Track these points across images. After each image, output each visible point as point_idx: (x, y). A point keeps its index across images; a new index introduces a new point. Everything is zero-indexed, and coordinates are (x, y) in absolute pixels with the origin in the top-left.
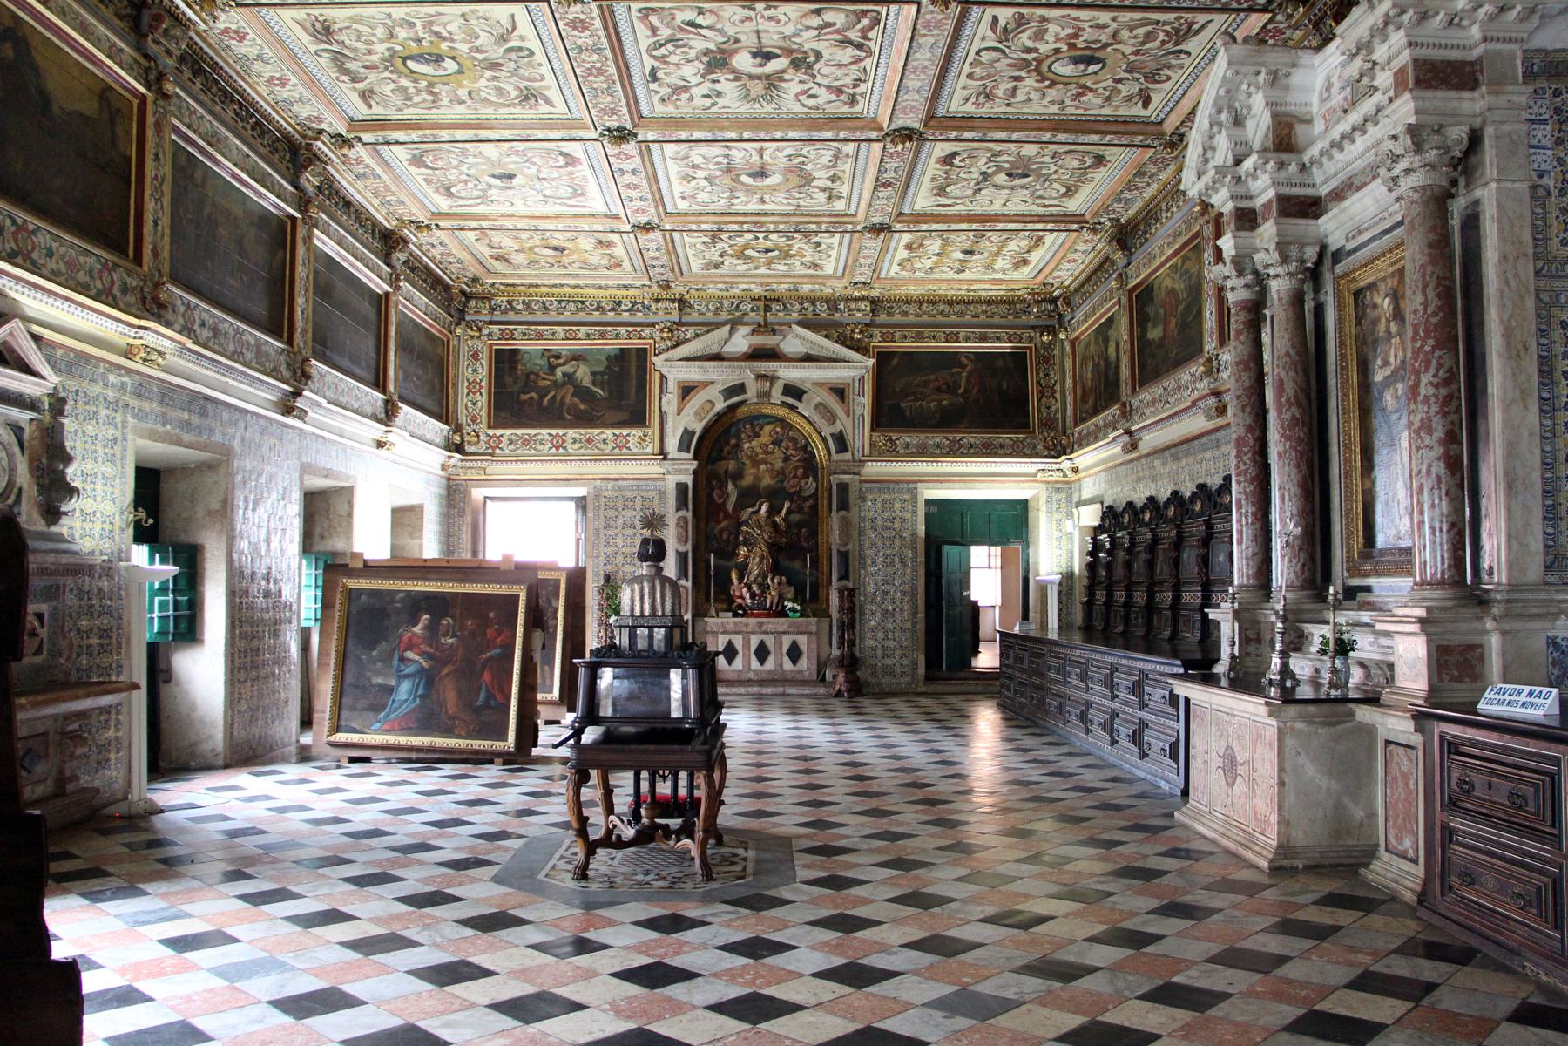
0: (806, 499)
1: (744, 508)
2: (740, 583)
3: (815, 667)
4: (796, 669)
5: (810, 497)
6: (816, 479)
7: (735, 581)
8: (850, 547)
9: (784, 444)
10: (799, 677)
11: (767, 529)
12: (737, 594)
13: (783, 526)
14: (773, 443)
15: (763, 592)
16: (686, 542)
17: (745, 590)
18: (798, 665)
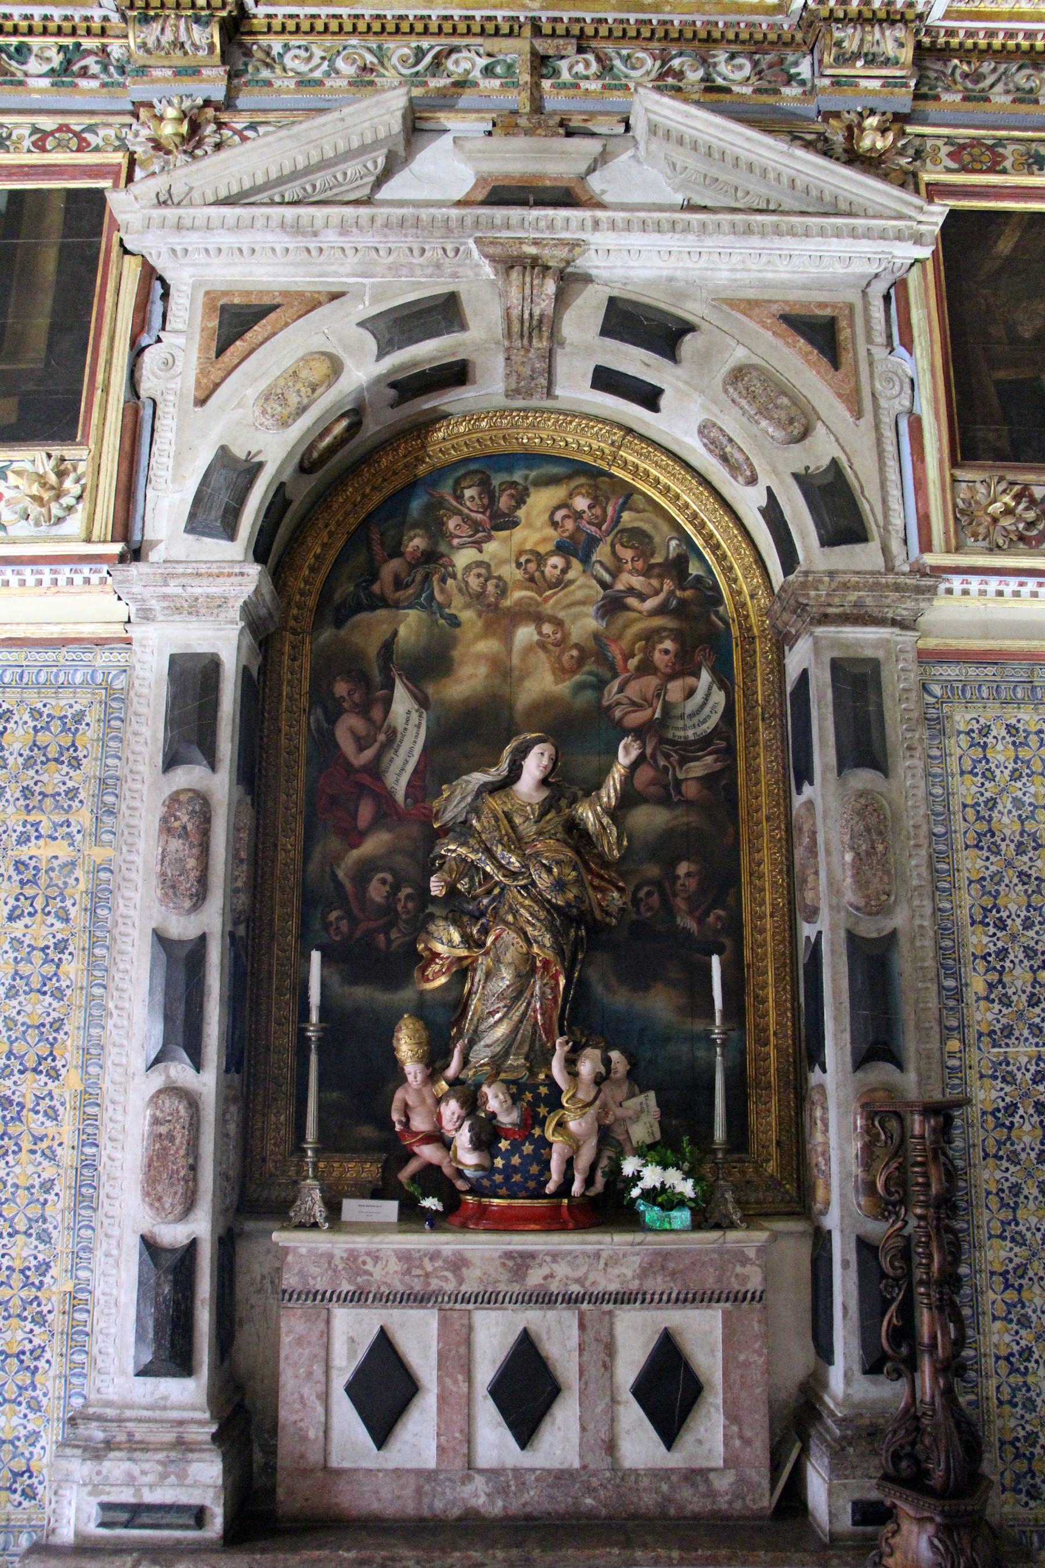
0: (688, 751)
1: (451, 774)
2: (433, 1073)
3: (759, 1452)
4: (675, 1460)
5: (705, 742)
6: (723, 678)
7: (413, 1070)
8: (899, 920)
9: (602, 553)
10: (691, 1500)
11: (549, 849)
12: (420, 1123)
13: (611, 845)
14: (561, 549)
15: (532, 1120)
16: (200, 896)
17: (451, 1109)
18: (687, 1441)
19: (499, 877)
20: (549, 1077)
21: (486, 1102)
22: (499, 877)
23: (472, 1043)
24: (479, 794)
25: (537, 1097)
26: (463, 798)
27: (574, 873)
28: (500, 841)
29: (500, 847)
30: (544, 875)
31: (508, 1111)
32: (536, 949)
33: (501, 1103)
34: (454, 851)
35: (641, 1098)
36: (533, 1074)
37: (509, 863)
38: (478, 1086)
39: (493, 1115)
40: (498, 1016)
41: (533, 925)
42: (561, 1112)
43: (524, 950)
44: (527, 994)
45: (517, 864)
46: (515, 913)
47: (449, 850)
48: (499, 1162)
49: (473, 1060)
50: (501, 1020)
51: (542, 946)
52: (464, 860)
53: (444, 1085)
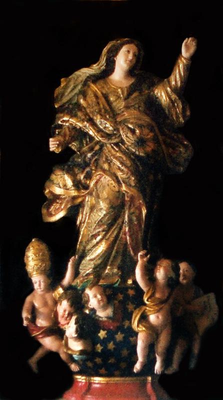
19: (98, 138)
20: (135, 282)
21: (88, 301)
22: (98, 138)
23: (82, 257)
24: (85, 83)
25: (127, 297)
26: (75, 87)
27: (151, 134)
28: (100, 112)
29: (99, 117)
30: (129, 135)
31: (105, 308)
32: (124, 188)
33: (99, 302)
34: (68, 121)
35: (204, 298)
36: (124, 280)
37: (105, 128)
38: (83, 290)
39: (93, 311)
40: (99, 238)
41: (122, 171)
42: (144, 307)
43: (117, 189)
44: (120, 221)
45: (111, 128)
46: (110, 163)
47: (64, 121)
48: (99, 348)
49: (82, 271)
50: (101, 240)
51: (128, 185)
52: (75, 128)
53: (60, 290)
